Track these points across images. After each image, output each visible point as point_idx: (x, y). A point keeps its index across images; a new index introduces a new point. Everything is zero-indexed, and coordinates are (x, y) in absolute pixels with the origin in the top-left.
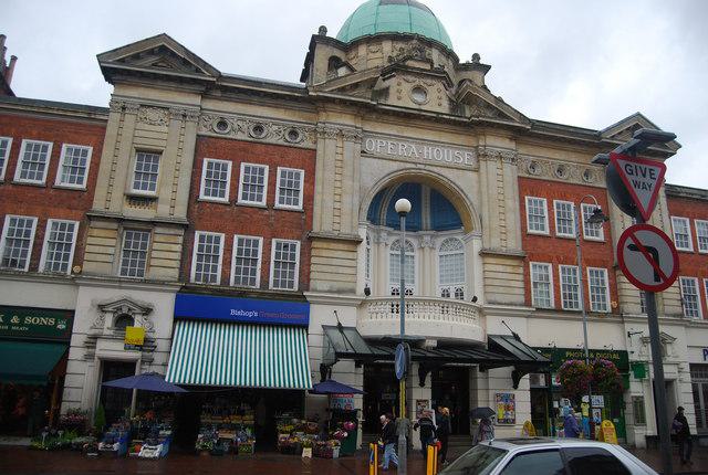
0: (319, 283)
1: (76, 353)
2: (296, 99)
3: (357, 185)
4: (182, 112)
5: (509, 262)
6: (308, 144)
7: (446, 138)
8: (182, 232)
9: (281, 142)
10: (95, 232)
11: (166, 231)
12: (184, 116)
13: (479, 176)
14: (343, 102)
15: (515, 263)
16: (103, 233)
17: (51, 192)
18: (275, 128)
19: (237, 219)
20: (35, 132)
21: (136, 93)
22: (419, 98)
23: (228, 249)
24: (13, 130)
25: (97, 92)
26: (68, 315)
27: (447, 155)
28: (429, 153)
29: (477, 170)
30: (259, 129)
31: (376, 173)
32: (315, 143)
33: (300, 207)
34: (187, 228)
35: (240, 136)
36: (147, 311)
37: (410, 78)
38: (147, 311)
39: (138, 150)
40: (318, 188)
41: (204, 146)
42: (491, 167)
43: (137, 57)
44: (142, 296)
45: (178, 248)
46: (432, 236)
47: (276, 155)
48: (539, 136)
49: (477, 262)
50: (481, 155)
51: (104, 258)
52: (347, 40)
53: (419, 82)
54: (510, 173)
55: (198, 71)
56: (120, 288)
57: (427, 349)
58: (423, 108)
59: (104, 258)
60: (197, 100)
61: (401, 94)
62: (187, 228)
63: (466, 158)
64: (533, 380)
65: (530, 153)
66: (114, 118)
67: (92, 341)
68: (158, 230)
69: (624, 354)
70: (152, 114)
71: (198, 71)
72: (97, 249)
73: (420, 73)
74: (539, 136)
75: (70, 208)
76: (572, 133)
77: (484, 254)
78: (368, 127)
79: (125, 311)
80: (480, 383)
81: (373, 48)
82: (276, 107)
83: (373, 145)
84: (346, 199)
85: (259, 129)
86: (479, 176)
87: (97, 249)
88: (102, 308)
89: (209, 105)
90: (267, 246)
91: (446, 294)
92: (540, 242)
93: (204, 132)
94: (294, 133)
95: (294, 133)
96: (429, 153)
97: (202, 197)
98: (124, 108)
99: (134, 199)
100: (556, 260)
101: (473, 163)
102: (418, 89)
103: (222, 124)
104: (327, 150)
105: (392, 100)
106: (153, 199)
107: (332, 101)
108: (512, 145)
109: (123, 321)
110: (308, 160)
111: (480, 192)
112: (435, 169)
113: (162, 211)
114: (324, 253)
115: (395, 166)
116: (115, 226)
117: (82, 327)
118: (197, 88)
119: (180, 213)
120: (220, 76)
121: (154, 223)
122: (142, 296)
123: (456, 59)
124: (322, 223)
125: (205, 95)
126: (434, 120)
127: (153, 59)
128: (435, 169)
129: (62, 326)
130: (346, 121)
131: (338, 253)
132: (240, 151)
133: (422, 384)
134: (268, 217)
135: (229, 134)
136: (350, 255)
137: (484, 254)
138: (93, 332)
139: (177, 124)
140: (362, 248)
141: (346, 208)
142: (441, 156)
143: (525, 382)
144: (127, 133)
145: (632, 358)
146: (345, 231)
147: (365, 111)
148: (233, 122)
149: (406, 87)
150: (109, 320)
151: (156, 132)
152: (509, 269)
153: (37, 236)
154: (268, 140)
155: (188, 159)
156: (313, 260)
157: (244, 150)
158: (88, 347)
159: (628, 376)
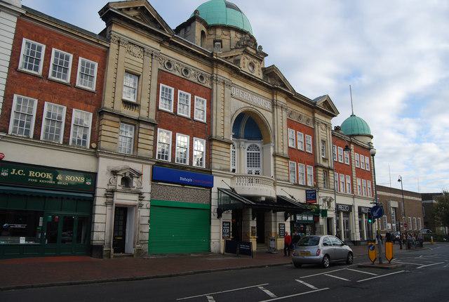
1: (100, 201)
2: (204, 57)
4: (150, 52)
5: (284, 160)
6: (208, 85)
8: (153, 128)
9: (196, 81)
10: (107, 122)
11: (146, 127)
12: (152, 55)
13: (273, 115)
14: (227, 65)
16: (110, 123)
17: (74, 90)
18: (193, 72)
20: (61, 45)
24: (46, 39)
25: (98, 26)
26: (93, 176)
31: (236, 107)
32: (212, 84)
35: (177, 73)
36: (140, 175)
38: (140, 175)
39: (127, 71)
43: (128, 9)
44: (136, 166)
46: (245, 142)
48: (295, 99)
49: (272, 158)
50: (274, 105)
51: (112, 140)
52: (210, 23)
55: (161, 28)
56: (124, 160)
57: (262, 202)
59: (112, 140)
60: (157, 46)
63: (268, 106)
64: (291, 218)
67: (111, 193)
68: (142, 125)
70: (136, 50)
72: (108, 134)
74: (295, 99)
75: (86, 103)
76: (307, 101)
77: (275, 155)
79: (127, 175)
80: (273, 218)
81: (225, 32)
82: (194, 59)
83: (236, 92)
86: (273, 115)
87: (108, 134)
88: (114, 173)
91: (250, 172)
94: (202, 77)
95: (202, 77)
98: (119, 42)
99: (126, 103)
100: (299, 161)
101: (270, 108)
103: (169, 64)
104: (219, 90)
107: (222, 63)
108: (285, 102)
109: (126, 181)
110: (209, 95)
111: (274, 124)
113: (144, 113)
114: (217, 148)
115: (243, 104)
116: (118, 119)
117: (103, 183)
118: (158, 38)
122: (136, 166)
125: (161, 44)
127: (134, 13)
129: (89, 183)
132: (179, 83)
133: (253, 219)
134: (192, 124)
135: (171, 70)
137: (275, 155)
138: (110, 187)
141: (226, 124)
142: (259, 101)
143: (289, 220)
144: (121, 59)
145: (321, 208)
150: (119, 178)
153: (66, 120)
154: (189, 79)
156: (213, 152)
157: (180, 82)
158: (107, 197)
159: (318, 216)
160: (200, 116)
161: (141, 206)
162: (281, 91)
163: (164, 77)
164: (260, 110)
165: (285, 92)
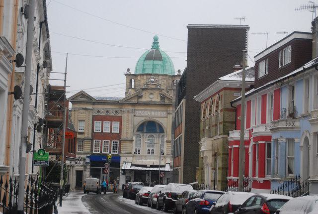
0: (123, 151)
3: (132, 125)
6: (120, 115)
7: (158, 108)
19: (102, 136)
21: (77, 106)
22: (151, 96)
23: (102, 144)
27: (158, 114)
28: (153, 113)
29: (167, 117)
30: (107, 112)
31: (138, 121)
33: (118, 132)
34: (92, 140)
37: (149, 91)
40: (122, 127)
41: (95, 118)
45: (90, 144)
47: (112, 119)
49: (165, 143)
53: (152, 91)
58: (153, 100)
61: (146, 98)
63: (164, 114)
66: (73, 113)
71: (91, 99)
73: (152, 89)
83: (137, 113)
84: (130, 130)
85: (107, 112)
89: (95, 106)
90: (111, 142)
93: (94, 114)
94: (116, 112)
95: (116, 112)
96: (153, 113)
97: (95, 131)
102: (151, 94)
103: (98, 112)
105: (144, 100)
106: (84, 133)
110: (120, 119)
112: (155, 118)
113: (86, 136)
115: (143, 119)
119: (90, 136)
120: (97, 100)
121: (84, 139)
124: (124, 136)
126: (155, 104)
128: (155, 118)
130: (130, 108)
131: (128, 144)
132: (103, 119)
136: (130, 144)
139: (87, 113)
140: (134, 143)
146: (129, 138)
147: (133, 104)
148: (101, 111)
149: (148, 94)
151: (83, 115)
154: (110, 115)
155: (91, 122)
160: (116, 131)
161: (86, 171)
163: (95, 118)
164: (157, 119)
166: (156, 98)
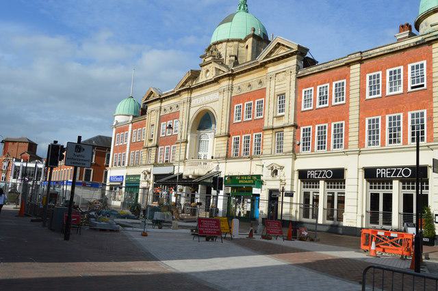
15: (223, 139)
42: (222, 95)
54: (227, 96)
62: (157, 146)
65: (238, 81)
69: (259, 176)
74: (238, 73)
78: (193, 95)
89: (163, 104)
92: (237, 125)
102: (208, 71)
123: (240, 41)
125: (161, 102)
130: (185, 96)
145: (262, 178)
152: (223, 142)
162: (223, 77)
165: (225, 76)
166: (211, 75)
